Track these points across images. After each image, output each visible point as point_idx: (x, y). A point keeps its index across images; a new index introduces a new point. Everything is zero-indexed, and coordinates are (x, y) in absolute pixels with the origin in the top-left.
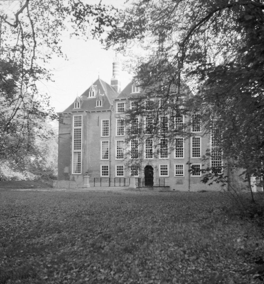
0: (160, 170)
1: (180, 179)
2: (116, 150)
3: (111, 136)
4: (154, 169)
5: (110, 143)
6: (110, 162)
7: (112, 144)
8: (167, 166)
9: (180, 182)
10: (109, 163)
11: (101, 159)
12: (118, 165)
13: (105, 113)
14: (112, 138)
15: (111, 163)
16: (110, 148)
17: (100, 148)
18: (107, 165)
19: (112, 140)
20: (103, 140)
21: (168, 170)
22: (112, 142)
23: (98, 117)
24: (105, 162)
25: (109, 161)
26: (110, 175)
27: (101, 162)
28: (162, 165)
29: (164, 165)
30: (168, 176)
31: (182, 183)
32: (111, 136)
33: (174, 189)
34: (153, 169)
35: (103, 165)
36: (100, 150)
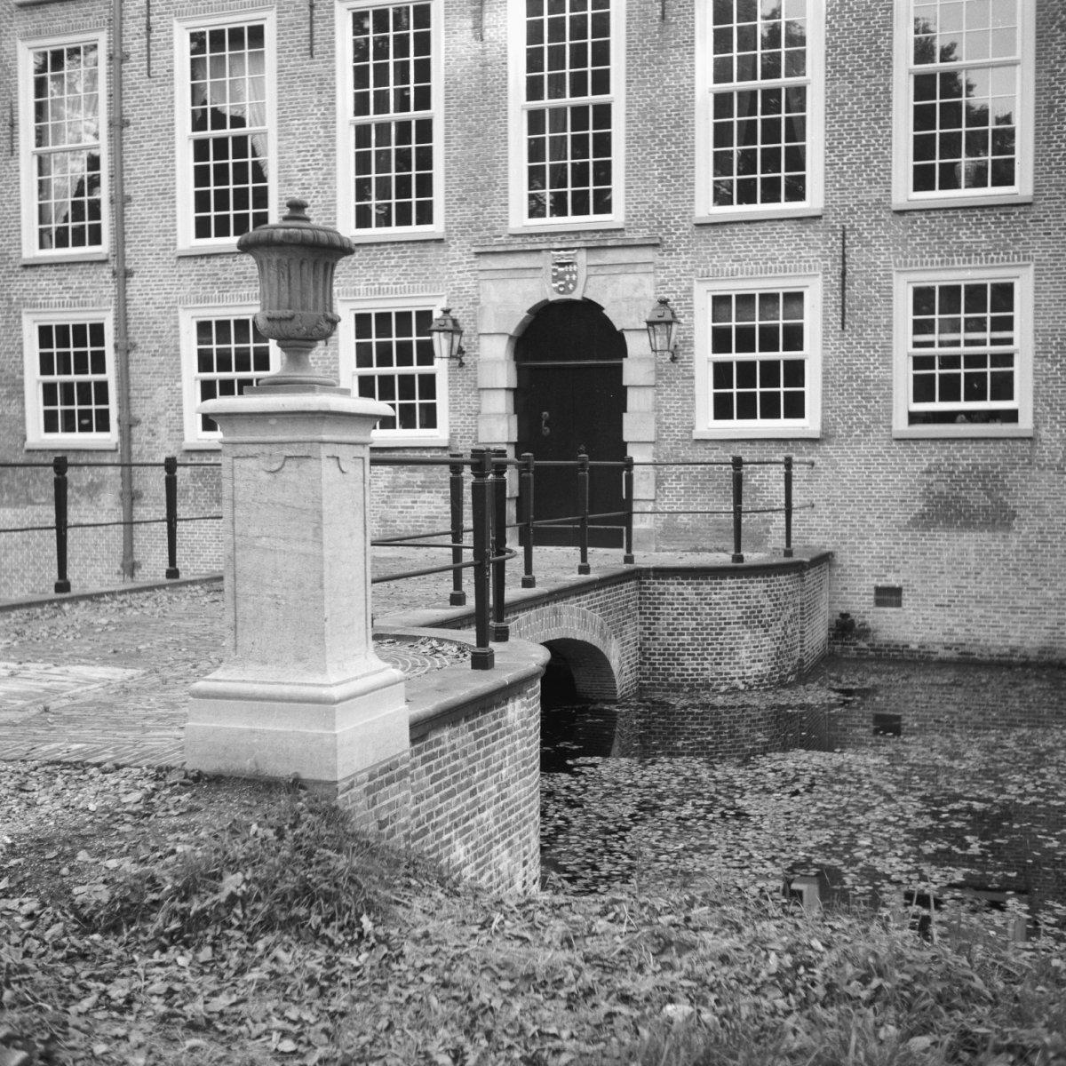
0: (704, 358)
1: (968, 457)
2: (184, 137)
4: (637, 345)
5: (118, 58)
7: (134, 71)
8: (795, 298)
9: (977, 498)
10: (110, 290)
11: (30, 249)
12: (214, 314)
15: (134, 284)
16: (119, 124)
17: (13, 125)
18: (86, 318)
19: (133, 27)
20: (39, 34)
21: (812, 353)
22: (135, 45)
24: (73, 279)
25: (106, 272)
26: (128, 425)
27: (29, 281)
28: (733, 288)
29: (756, 287)
30: (810, 424)
31: (999, 518)
33: (892, 580)
34: (615, 343)
35: (55, 319)
36: (13, 151)
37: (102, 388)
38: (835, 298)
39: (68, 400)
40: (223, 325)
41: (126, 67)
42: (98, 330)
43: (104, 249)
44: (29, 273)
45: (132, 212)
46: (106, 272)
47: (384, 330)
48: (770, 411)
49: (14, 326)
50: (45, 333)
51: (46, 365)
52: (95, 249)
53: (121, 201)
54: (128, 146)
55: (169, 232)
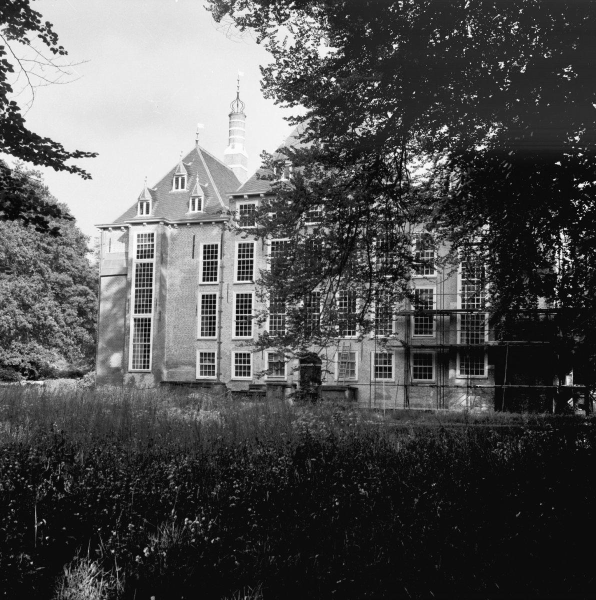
3: (222, 282)
5: (221, 298)
6: (220, 343)
7: (224, 301)
10: (217, 346)
11: (199, 337)
12: (239, 352)
13: (209, 228)
14: (225, 285)
15: (222, 345)
16: (220, 312)
18: (211, 351)
19: (225, 292)
22: (225, 295)
23: (194, 236)
24: (208, 343)
26: (219, 375)
32: (222, 282)
37: (214, 366)
38: (360, 355)
39: (206, 369)
40: (241, 354)
41: (223, 300)
42: (213, 354)
43: (216, 337)
44: (199, 342)
45: (222, 330)
46: (216, 342)
47: (241, 357)
48: (245, 375)
49: (194, 353)
50: (201, 354)
51: (236, 362)
52: (250, 337)
53: (220, 328)
54: (222, 316)
55: (230, 335)
